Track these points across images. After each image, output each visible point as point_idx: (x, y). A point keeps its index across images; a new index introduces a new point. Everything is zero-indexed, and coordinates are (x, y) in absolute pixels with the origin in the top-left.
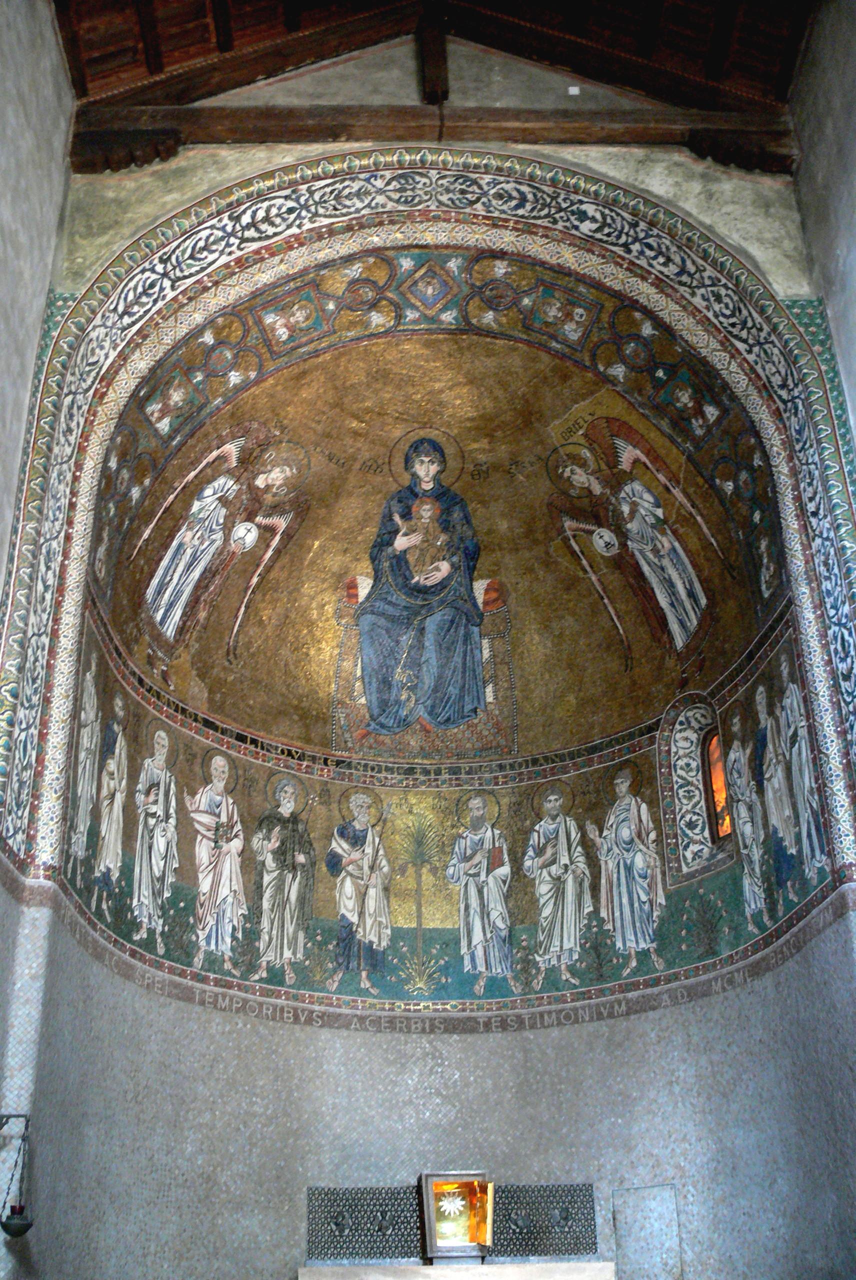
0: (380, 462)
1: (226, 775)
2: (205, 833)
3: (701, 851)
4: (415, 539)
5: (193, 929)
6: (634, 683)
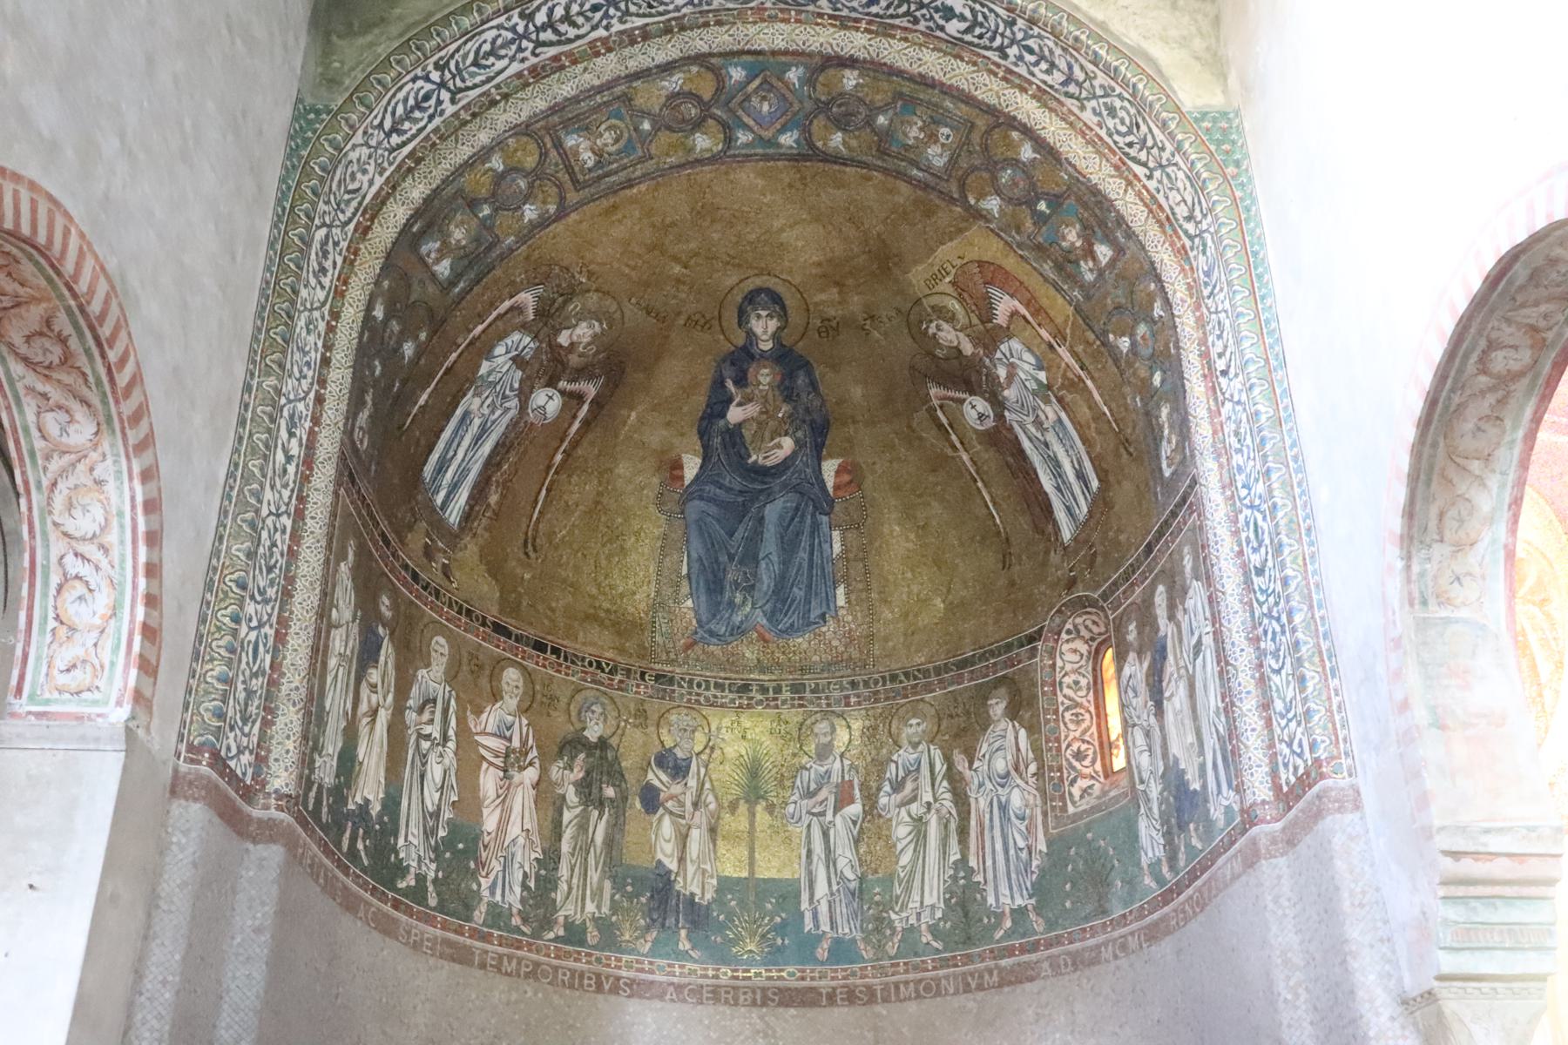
0: (708, 316)
1: (521, 691)
2: (492, 759)
3: (1091, 787)
4: (752, 410)
5: (474, 875)
6: (1012, 584)
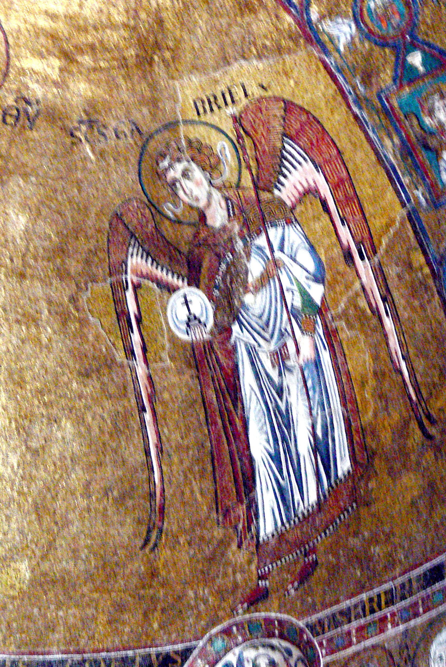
6: (154, 574)
